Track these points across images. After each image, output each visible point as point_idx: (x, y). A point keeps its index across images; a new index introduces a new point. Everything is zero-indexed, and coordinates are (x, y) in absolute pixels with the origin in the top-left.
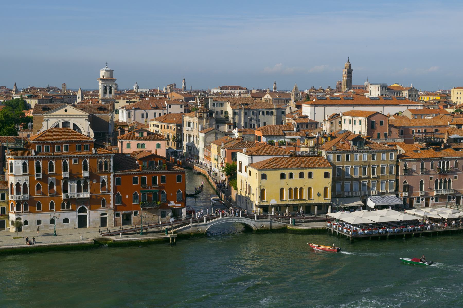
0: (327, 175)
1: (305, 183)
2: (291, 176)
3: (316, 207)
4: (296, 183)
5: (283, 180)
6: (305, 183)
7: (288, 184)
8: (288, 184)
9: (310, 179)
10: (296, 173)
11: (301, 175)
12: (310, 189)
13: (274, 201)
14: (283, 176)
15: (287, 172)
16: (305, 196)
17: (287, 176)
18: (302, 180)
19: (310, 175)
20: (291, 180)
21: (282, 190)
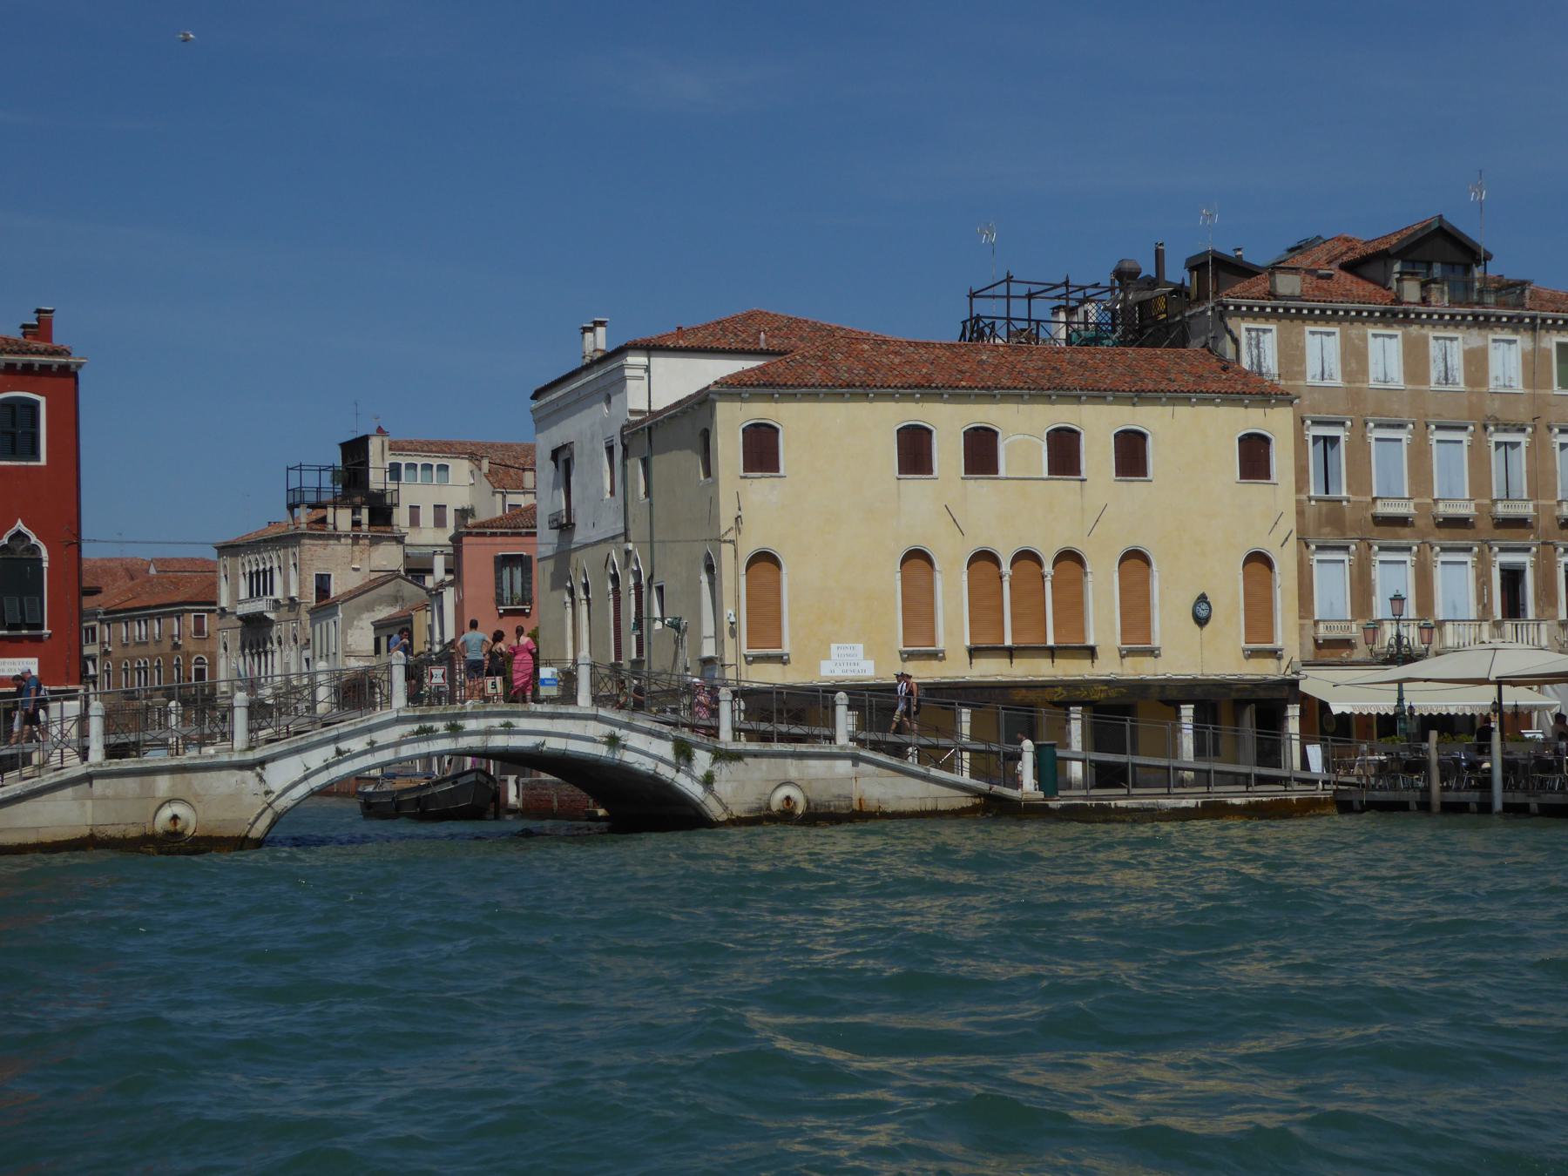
0: (1254, 457)
1: (1090, 514)
2: (981, 452)
3: (1187, 711)
4: (1022, 510)
5: (915, 485)
6: (1090, 514)
7: (961, 515)
8: (961, 515)
9: (1134, 488)
10: (1022, 428)
11: (1064, 452)
12: (1135, 559)
13: (849, 661)
14: (915, 451)
15: (948, 422)
16: (1102, 621)
17: (948, 452)
18: (1064, 487)
19: (1131, 454)
20: (981, 486)
21: (917, 558)
